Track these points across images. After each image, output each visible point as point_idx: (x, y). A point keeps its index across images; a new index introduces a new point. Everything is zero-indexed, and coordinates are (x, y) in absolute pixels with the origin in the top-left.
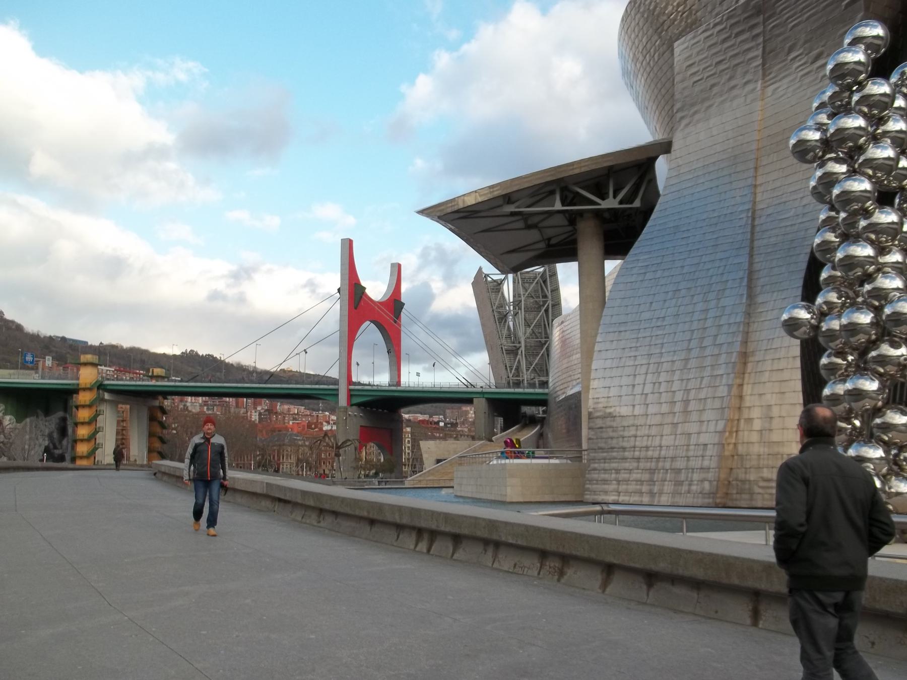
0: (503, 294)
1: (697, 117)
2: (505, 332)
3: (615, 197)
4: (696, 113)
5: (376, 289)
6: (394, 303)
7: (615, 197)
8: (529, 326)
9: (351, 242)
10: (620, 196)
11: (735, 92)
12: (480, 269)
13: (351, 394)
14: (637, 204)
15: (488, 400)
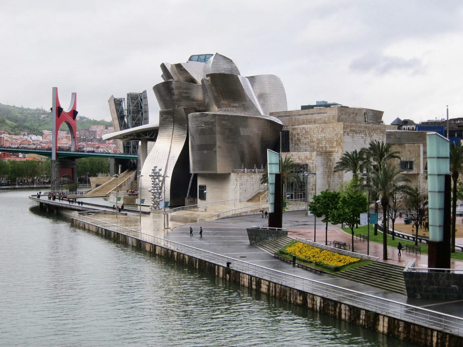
0: (122, 107)
1: (163, 127)
2: (123, 124)
3: (149, 135)
4: (163, 126)
5: (66, 108)
6: (74, 113)
7: (149, 135)
8: (134, 120)
9: (57, 88)
10: (150, 135)
11: (169, 125)
12: (113, 96)
13: (57, 155)
14: (154, 137)
15: (115, 159)
